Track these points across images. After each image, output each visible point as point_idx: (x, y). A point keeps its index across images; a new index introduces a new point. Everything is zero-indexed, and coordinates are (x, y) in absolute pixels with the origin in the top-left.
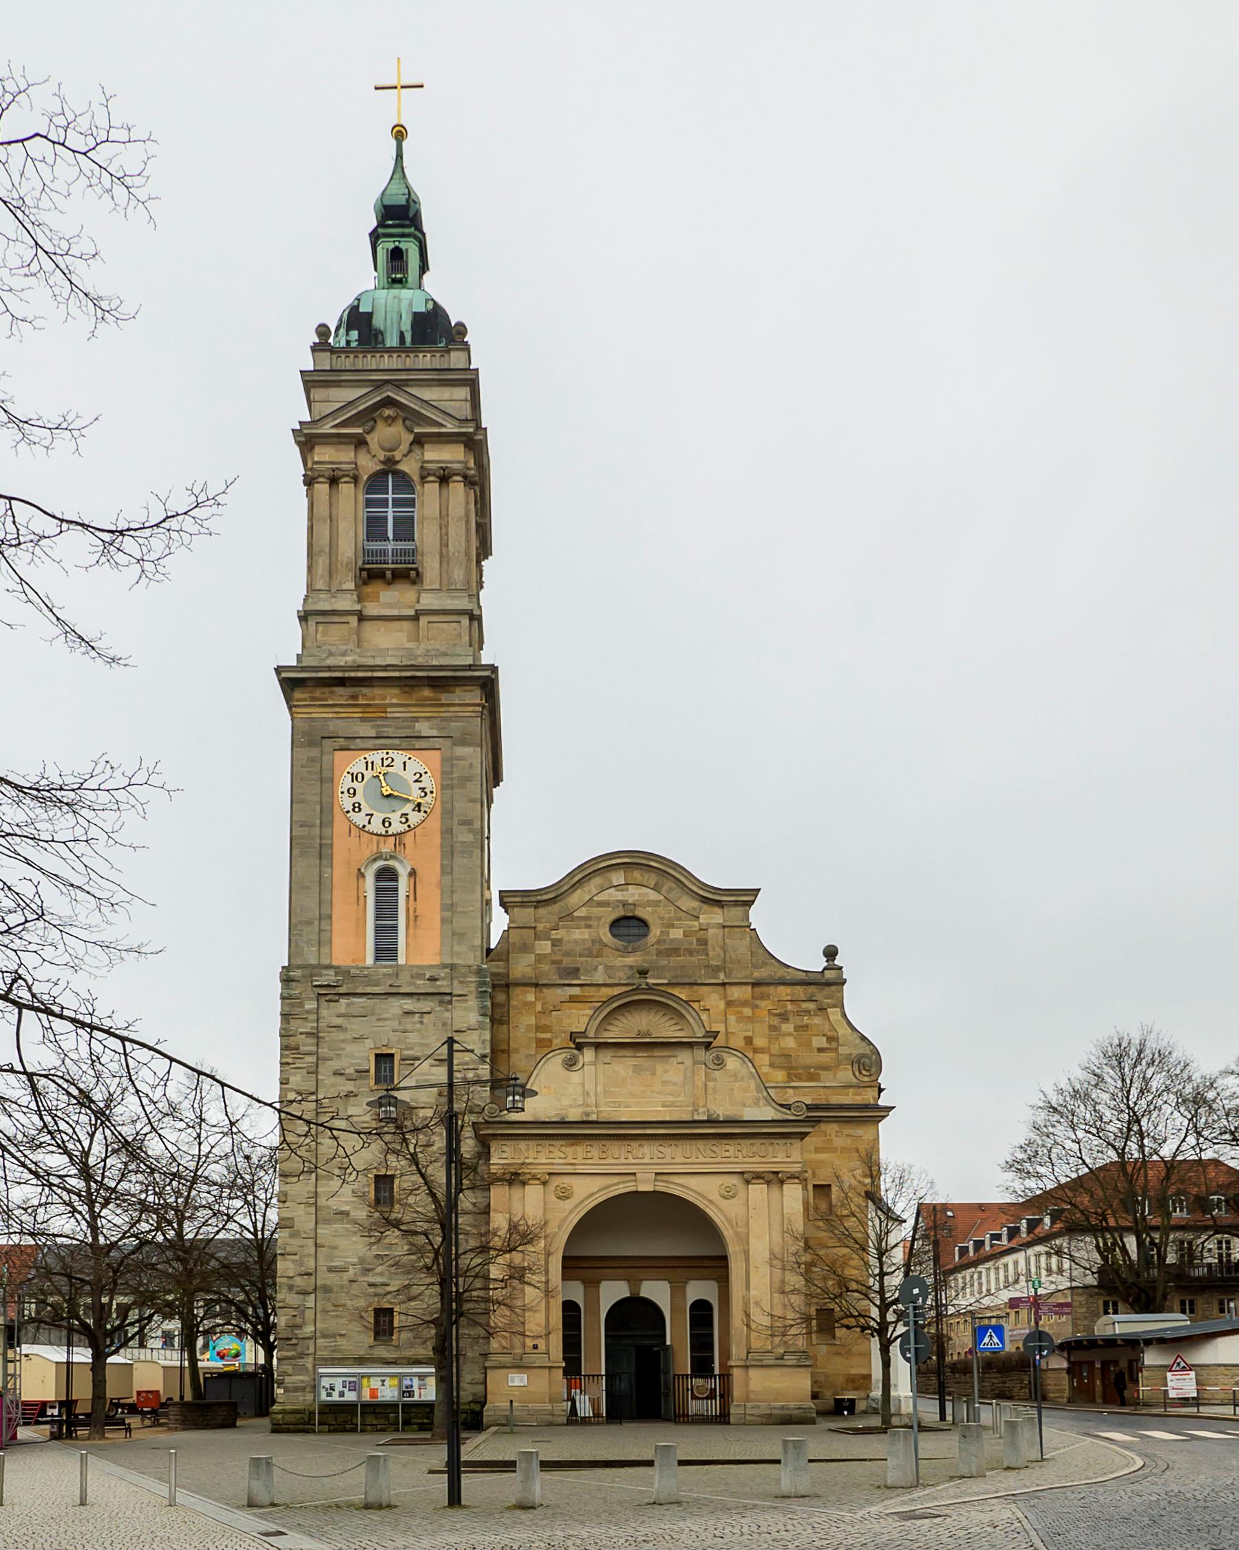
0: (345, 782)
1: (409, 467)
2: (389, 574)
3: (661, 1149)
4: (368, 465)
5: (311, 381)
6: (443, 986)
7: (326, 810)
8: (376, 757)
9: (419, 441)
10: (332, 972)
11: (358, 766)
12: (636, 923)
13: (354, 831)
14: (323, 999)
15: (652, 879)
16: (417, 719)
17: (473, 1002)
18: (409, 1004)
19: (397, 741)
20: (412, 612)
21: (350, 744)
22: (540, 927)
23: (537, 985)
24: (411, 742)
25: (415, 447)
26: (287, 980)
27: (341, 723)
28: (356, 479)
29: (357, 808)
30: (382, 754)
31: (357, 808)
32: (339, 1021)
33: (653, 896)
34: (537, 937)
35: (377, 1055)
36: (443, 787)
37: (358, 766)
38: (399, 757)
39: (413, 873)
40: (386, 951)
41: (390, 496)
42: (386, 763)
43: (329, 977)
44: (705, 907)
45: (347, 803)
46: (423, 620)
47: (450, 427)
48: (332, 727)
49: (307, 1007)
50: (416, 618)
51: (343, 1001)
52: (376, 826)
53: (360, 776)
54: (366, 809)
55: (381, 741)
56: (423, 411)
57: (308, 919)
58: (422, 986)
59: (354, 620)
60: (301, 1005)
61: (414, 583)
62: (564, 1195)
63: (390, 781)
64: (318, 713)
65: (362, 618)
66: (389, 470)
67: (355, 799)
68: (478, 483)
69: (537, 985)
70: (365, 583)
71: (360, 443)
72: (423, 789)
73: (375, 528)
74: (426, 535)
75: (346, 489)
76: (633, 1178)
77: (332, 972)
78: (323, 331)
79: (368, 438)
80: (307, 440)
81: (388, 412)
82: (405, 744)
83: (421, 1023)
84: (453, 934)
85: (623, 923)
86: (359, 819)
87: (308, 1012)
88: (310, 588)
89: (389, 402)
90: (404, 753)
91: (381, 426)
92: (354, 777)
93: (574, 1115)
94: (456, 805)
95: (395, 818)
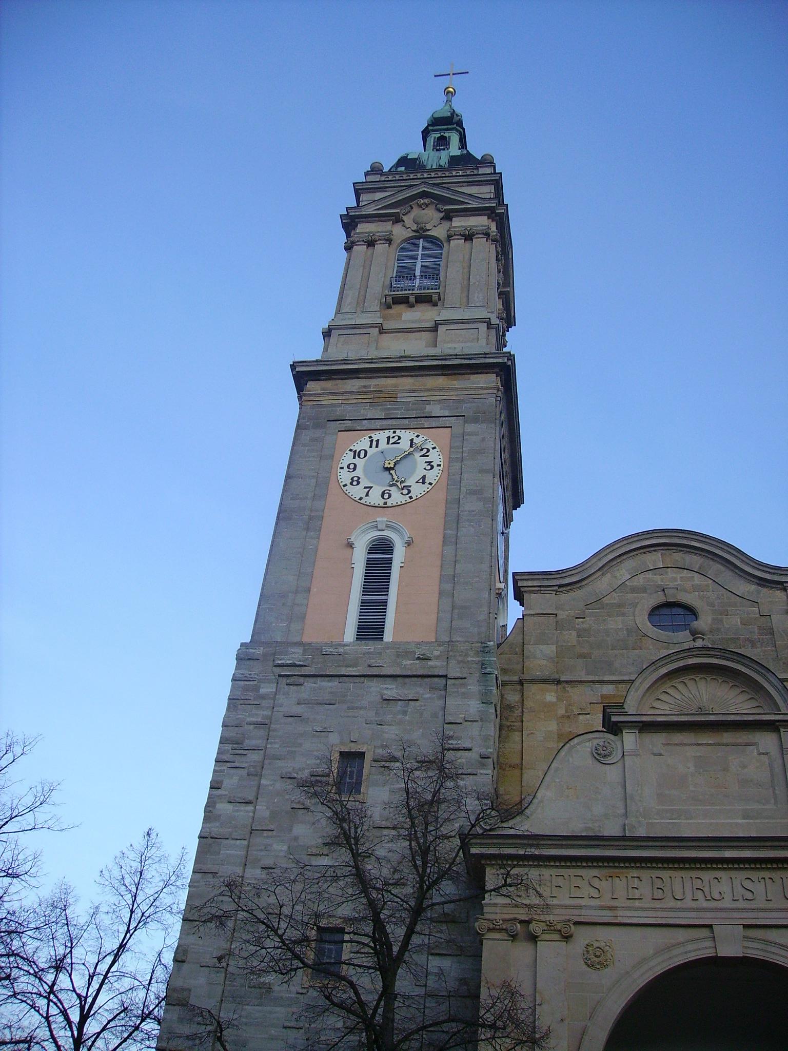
2: (412, 299)
3: (748, 884)
6: (437, 666)
7: (322, 485)
8: (382, 436)
9: (448, 217)
10: (300, 650)
11: (362, 444)
12: (680, 611)
14: (284, 681)
15: (695, 560)
16: (428, 402)
17: (473, 687)
18: (391, 689)
19: (406, 422)
21: (355, 425)
22: (562, 615)
23: (559, 682)
24: (420, 420)
26: (244, 657)
27: (349, 408)
28: (389, 241)
30: (390, 433)
31: (356, 481)
32: (298, 710)
33: (698, 579)
34: (559, 626)
35: (342, 754)
36: (451, 460)
39: (409, 544)
40: (371, 629)
41: (420, 253)
42: (392, 441)
43: (295, 655)
44: (764, 591)
45: (345, 476)
46: (441, 329)
48: (339, 412)
49: (263, 691)
50: (435, 329)
51: (309, 684)
52: (375, 498)
53: (362, 453)
54: (364, 482)
55: (391, 422)
57: (281, 597)
58: (409, 665)
59: (376, 331)
60: (256, 689)
61: (435, 305)
62: (596, 959)
63: (400, 472)
64: (326, 400)
65: (382, 331)
66: (421, 233)
67: (353, 474)
68: (503, 243)
69: (559, 682)
70: (389, 307)
71: (397, 219)
72: (429, 463)
74: (452, 274)
75: (380, 248)
76: (705, 932)
77: (300, 650)
80: (350, 222)
82: (414, 423)
83: (405, 713)
84: (453, 608)
85: (665, 611)
86: (357, 492)
87: (263, 697)
88: (338, 312)
90: (412, 432)
91: (416, 212)
92: (356, 454)
93: (612, 829)
94: (465, 476)
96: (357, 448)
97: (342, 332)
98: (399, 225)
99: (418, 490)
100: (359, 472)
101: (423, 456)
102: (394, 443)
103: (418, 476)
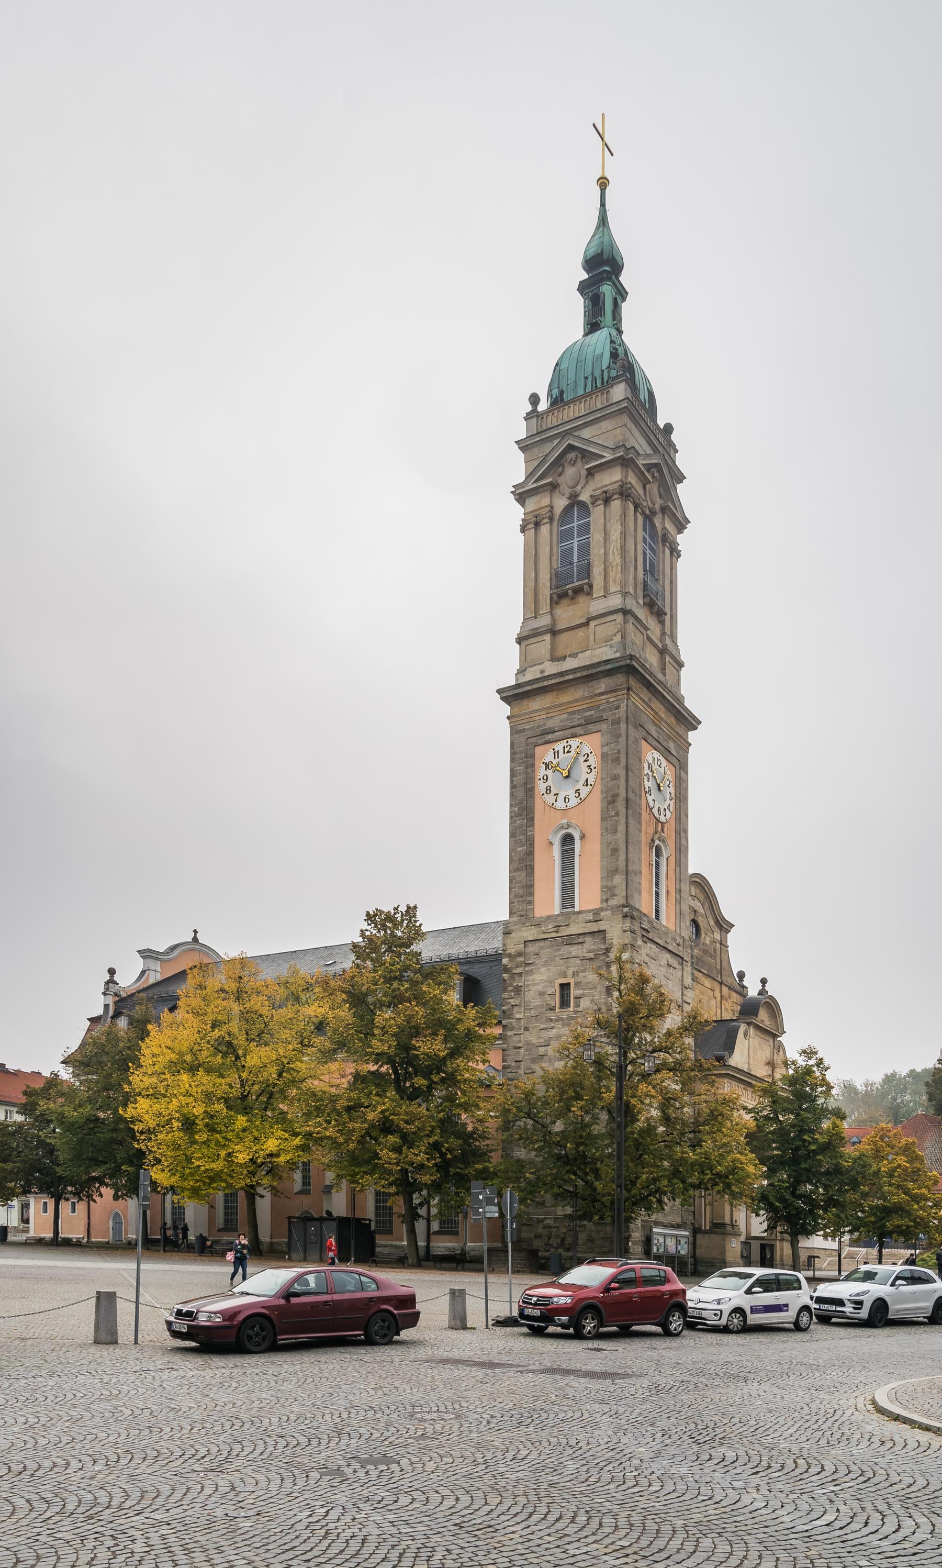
0: (541, 771)
1: (584, 497)
2: (570, 592)
4: (561, 503)
5: (524, 446)
8: (559, 746)
9: (591, 473)
13: (547, 808)
20: (583, 620)
25: (589, 477)
29: (548, 790)
30: (564, 743)
37: (549, 757)
38: (574, 743)
39: (583, 837)
46: (592, 624)
47: (609, 456)
52: (560, 804)
54: (554, 791)
56: (590, 449)
59: (548, 637)
65: (554, 632)
67: (546, 784)
71: (554, 487)
73: (566, 555)
75: (545, 529)
78: (534, 399)
79: (560, 480)
81: (571, 456)
89: (571, 448)
95: (571, 794)
96: (547, 761)
97: (529, 641)
98: (556, 494)
99: (584, 791)
100: (550, 783)
101: (586, 761)
102: (568, 752)
103: (583, 781)
